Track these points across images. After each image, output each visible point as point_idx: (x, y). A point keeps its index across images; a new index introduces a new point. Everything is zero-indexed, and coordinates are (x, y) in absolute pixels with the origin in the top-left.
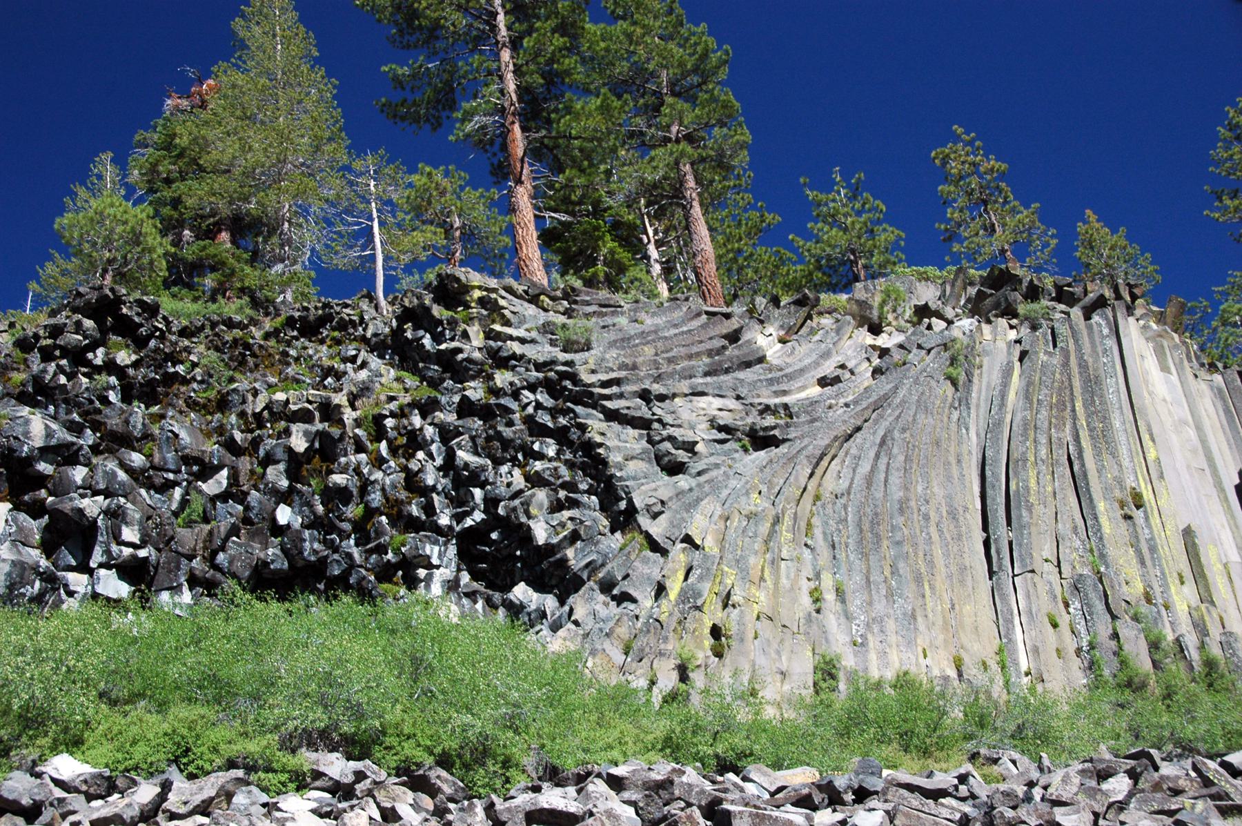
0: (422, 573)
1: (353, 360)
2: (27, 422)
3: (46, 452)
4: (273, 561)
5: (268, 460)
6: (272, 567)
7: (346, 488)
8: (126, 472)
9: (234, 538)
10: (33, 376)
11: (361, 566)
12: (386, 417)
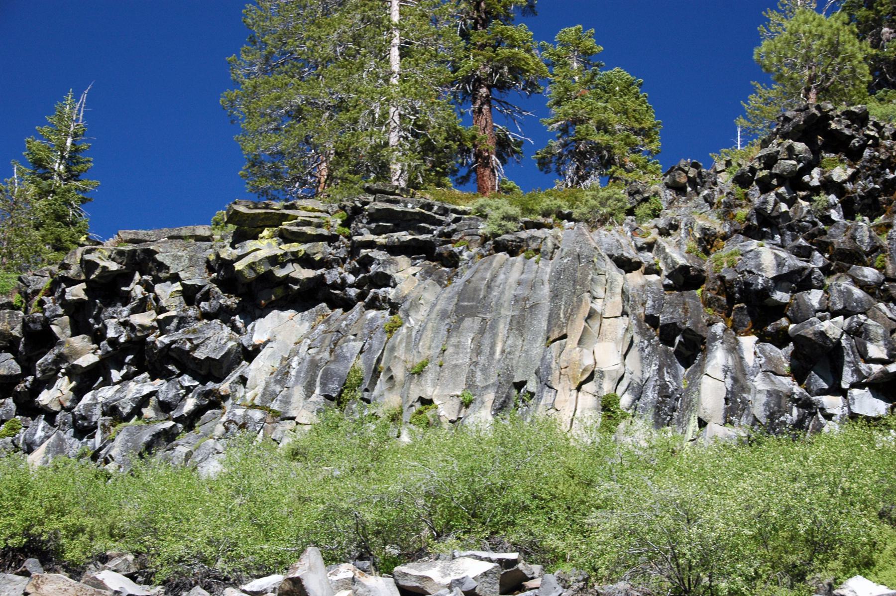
2: (757, 255)
3: (780, 281)
8: (861, 288)
10: (755, 209)
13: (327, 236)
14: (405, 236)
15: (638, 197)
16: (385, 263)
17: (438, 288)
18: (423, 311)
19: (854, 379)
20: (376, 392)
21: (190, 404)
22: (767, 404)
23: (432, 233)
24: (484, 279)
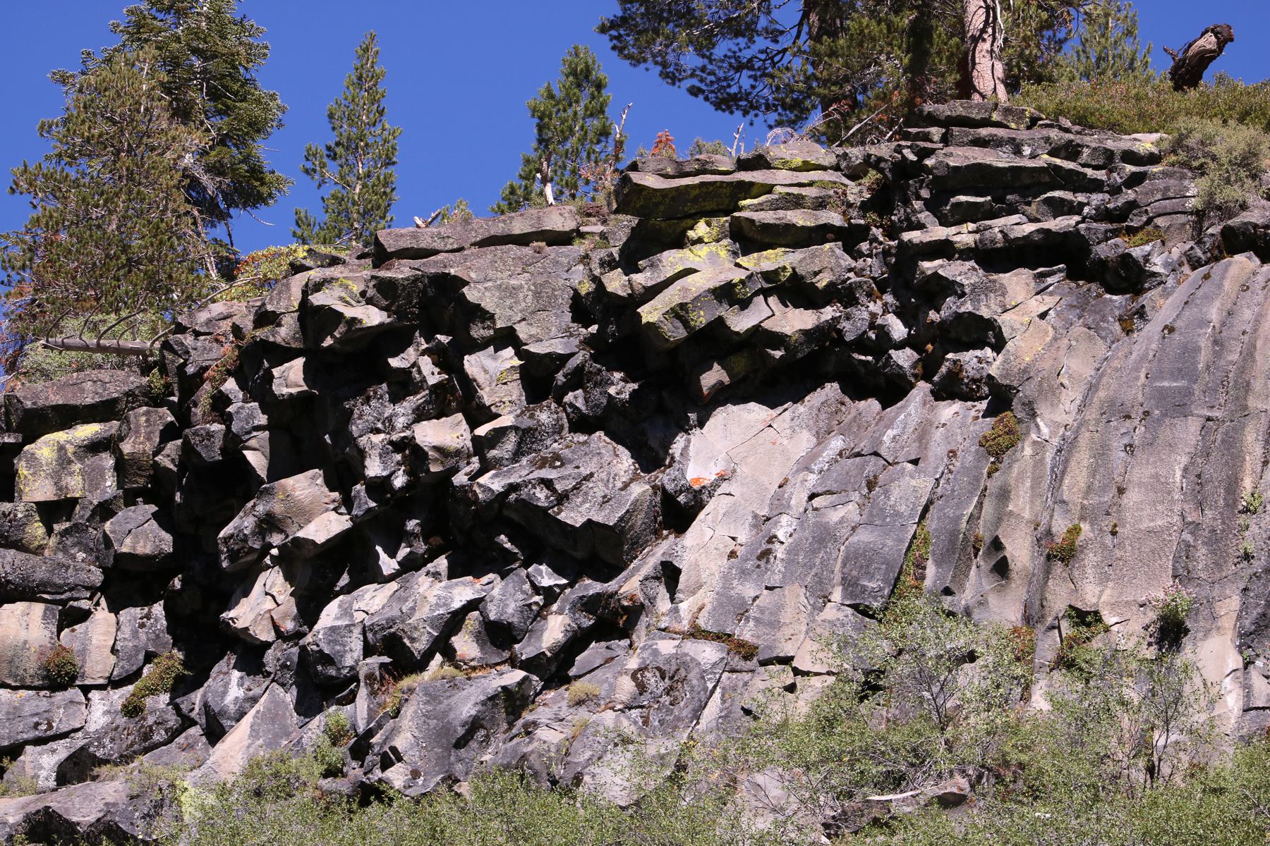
13: (840, 228)
14: (1018, 226)
16: (980, 291)
17: (1101, 348)
18: (1070, 399)
20: (966, 597)
21: (554, 630)
23: (1079, 213)
24: (1205, 323)
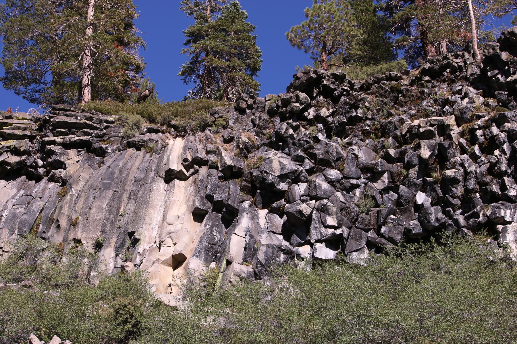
0: (500, 227)
1: (459, 92)
2: (271, 161)
3: (282, 178)
4: (414, 229)
5: (408, 166)
6: (413, 232)
7: (454, 177)
9: (392, 216)
10: (275, 132)
11: (464, 227)
12: (476, 129)
13: (29, 136)
14: (74, 138)
15: (217, 116)
17: (92, 171)
18: (81, 184)
19: (319, 237)
20: (49, 234)
22: (266, 253)
23: (91, 135)
24: (118, 166)
